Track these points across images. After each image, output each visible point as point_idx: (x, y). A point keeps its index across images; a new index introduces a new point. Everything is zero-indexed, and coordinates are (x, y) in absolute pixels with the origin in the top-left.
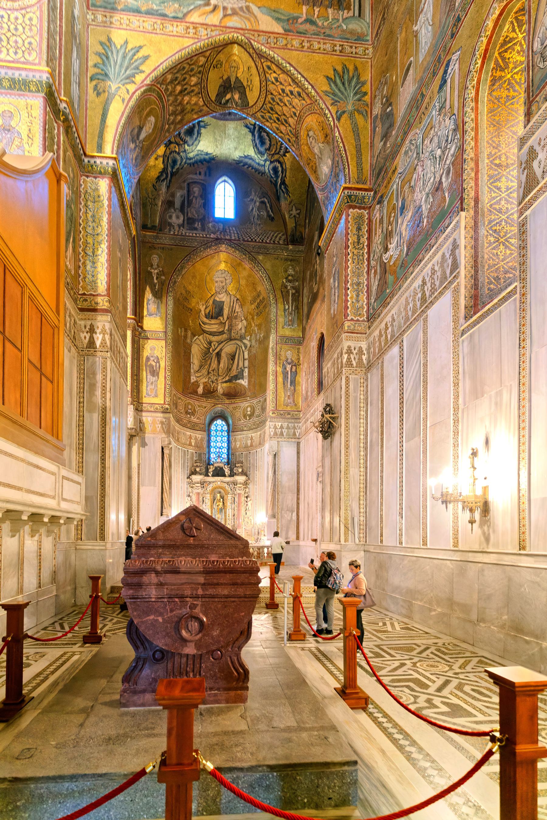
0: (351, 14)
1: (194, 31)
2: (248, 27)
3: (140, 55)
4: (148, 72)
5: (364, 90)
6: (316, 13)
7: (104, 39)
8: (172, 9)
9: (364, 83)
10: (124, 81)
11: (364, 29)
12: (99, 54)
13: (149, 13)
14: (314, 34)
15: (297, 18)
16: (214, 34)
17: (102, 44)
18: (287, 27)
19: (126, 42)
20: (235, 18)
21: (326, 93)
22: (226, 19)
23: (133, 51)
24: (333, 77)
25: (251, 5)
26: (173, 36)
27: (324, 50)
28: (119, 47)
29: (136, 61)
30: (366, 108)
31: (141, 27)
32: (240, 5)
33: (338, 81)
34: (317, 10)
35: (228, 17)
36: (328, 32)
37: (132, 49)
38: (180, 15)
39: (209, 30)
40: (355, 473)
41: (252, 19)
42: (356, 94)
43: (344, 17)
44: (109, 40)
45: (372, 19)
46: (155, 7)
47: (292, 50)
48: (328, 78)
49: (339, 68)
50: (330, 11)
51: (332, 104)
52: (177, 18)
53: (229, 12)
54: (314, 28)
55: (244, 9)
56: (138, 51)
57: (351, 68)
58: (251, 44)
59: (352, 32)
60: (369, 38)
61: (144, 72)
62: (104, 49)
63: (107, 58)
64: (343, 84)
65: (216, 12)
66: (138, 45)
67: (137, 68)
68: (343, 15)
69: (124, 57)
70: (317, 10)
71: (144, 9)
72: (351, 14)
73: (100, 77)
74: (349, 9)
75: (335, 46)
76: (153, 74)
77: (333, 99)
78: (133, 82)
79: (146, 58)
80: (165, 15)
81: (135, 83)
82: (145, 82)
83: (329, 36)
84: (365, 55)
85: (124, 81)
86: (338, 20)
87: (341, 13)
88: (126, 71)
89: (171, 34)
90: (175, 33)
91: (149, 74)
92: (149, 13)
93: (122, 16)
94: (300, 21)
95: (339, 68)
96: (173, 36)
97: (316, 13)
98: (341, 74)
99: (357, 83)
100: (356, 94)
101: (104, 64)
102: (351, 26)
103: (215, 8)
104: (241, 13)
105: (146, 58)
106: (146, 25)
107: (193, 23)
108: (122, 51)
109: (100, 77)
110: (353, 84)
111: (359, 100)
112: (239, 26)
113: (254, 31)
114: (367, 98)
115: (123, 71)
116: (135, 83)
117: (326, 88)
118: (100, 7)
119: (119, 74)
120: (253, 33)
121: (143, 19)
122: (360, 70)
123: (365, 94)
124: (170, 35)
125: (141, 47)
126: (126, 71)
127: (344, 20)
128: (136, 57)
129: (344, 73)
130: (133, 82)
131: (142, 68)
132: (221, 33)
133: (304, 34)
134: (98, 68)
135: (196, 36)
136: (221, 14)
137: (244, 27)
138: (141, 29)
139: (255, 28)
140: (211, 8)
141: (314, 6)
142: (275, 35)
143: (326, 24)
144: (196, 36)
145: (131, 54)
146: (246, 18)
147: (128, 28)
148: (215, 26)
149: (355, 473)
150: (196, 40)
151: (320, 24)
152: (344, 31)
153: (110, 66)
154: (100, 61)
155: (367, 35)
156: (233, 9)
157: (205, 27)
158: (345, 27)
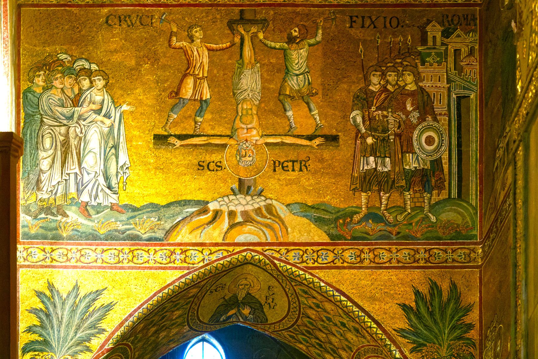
0: (444, 195)
1: (183, 256)
2: (269, 241)
3: (98, 304)
4: (110, 330)
5: (467, 320)
6: (384, 202)
7: (42, 287)
8: (147, 225)
9: (468, 309)
10: (74, 349)
11: (468, 219)
12: (34, 311)
13: (111, 237)
14: (381, 237)
15: (352, 214)
16: (213, 257)
17: (39, 294)
18: (333, 232)
19: (76, 287)
20: (249, 227)
21: (401, 332)
22: (233, 231)
23: (87, 300)
24: (413, 305)
25: (274, 203)
26: (151, 268)
27: (398, 262)
28: (64, 296)
29: (91, 315)
30: (472, 350)
31: (100, 261)
32: (256, 206)
33: (423, 310)
34: (384, 197)
35: (238, 228)
36: (405, 231)
37: (85, 297)
38: (160, 234)
39: (206, 252)
40: (523, 297)
41: (276, 226)
42: (454, 328)
43: (433, 202)
44: (51, 287)
45: (481, 200)
46: (121, 227)
47: (344, 268)
48: (405, 307)
49: (424, 290)
50: (408, 195)
51: (411, 351)
52: (156, 239)
53: (239, 219)
54: (381, 226)
55: (264, 211)
56: (94, 300)
57: (445, 286)
58: (275, 265)
59: (448, 225)
60: (476, 232)
61: (104, 330)
62: (43, 302)
63: (48, 315)
64: (431, 314)
65: (218, 220)
66: (94, 290)
67: (93, 326)
68: (430, 199)
69: (73, 311)
70: (384, 197)
71: (102, 232)
72: (444, 195)
73: (37, 347)
74: (440, 188)
75: (417, 251)
76: (119, 333)
77: (414, 342)
78: (88, 349)
79: (109, 307)
80: (135, 238)
81: (90, 351)
82: (106, 347)
83: (406, 237)
84: (469, 262)
85: (74, 349)
86: (422, 208)
87: (427, 195)
88: (76, 333)
89: (146, 265)
90: (151, 264)
91: (113, 333)
92: (111, 237)
93: (69, 247)
94: (356, 218)
95: (424, 290)
96: (151, 268)
97: (384, 202)
98: (428, 297)
99: (456, 310)
100: (454, 328)
101: (43, 327)
102: (444, 217)
103: (217, 214)
104: (259, 219)
105: (109, 307)
106: (106, 256)
107: (180, 244)
108: (70, 301)
109: (37, 347)
110: (449, 312)
111: (459, 338)
112: (256, 240)
113: (281, 244)
114: (474, 334)
115: (72, 334)
116: (90, 351)
117: (403, 324)
118: (36, 237)
119: (65, 339)
120: (277, 248)
121: (100, 248)
122: (461, 288)
123: (470, 327)
124: (146, 268)
125: (98, 293)
126: (76, 333)
127: (432, 207)
128: (91, 309)
129: (432, 295)
130: (88, 349)
131: (103, 325)
132: (225, 254)
133: (364, 238)
134: (34, 332)
135: (185, 265)
136: (225, 224)
137: (264, 240)
138: (99, 263)
139: (281, 240)
140: (210, 215)
141: (379, 191)
142: (315, 248)
143: (400, 218)
144: (185, 265)
145: (83, 305)
146: (267, 226)
147: (79, 264)
148: (216, 245)
149: (523, 297)
150: (186, 271)
151: (391, 219)
152: (433, 225)
153: (52, 327)
154: (36, 322)
155: (473, 228)
156: (245, 214)
157: (200, 248)
158: (433, 219)
